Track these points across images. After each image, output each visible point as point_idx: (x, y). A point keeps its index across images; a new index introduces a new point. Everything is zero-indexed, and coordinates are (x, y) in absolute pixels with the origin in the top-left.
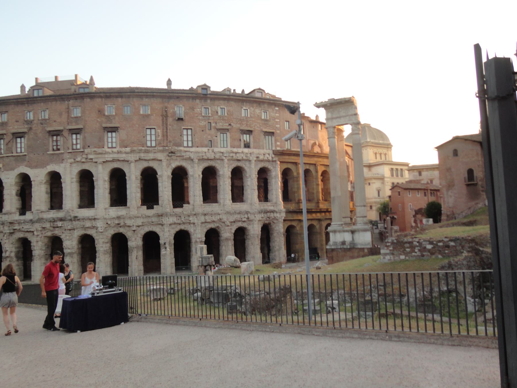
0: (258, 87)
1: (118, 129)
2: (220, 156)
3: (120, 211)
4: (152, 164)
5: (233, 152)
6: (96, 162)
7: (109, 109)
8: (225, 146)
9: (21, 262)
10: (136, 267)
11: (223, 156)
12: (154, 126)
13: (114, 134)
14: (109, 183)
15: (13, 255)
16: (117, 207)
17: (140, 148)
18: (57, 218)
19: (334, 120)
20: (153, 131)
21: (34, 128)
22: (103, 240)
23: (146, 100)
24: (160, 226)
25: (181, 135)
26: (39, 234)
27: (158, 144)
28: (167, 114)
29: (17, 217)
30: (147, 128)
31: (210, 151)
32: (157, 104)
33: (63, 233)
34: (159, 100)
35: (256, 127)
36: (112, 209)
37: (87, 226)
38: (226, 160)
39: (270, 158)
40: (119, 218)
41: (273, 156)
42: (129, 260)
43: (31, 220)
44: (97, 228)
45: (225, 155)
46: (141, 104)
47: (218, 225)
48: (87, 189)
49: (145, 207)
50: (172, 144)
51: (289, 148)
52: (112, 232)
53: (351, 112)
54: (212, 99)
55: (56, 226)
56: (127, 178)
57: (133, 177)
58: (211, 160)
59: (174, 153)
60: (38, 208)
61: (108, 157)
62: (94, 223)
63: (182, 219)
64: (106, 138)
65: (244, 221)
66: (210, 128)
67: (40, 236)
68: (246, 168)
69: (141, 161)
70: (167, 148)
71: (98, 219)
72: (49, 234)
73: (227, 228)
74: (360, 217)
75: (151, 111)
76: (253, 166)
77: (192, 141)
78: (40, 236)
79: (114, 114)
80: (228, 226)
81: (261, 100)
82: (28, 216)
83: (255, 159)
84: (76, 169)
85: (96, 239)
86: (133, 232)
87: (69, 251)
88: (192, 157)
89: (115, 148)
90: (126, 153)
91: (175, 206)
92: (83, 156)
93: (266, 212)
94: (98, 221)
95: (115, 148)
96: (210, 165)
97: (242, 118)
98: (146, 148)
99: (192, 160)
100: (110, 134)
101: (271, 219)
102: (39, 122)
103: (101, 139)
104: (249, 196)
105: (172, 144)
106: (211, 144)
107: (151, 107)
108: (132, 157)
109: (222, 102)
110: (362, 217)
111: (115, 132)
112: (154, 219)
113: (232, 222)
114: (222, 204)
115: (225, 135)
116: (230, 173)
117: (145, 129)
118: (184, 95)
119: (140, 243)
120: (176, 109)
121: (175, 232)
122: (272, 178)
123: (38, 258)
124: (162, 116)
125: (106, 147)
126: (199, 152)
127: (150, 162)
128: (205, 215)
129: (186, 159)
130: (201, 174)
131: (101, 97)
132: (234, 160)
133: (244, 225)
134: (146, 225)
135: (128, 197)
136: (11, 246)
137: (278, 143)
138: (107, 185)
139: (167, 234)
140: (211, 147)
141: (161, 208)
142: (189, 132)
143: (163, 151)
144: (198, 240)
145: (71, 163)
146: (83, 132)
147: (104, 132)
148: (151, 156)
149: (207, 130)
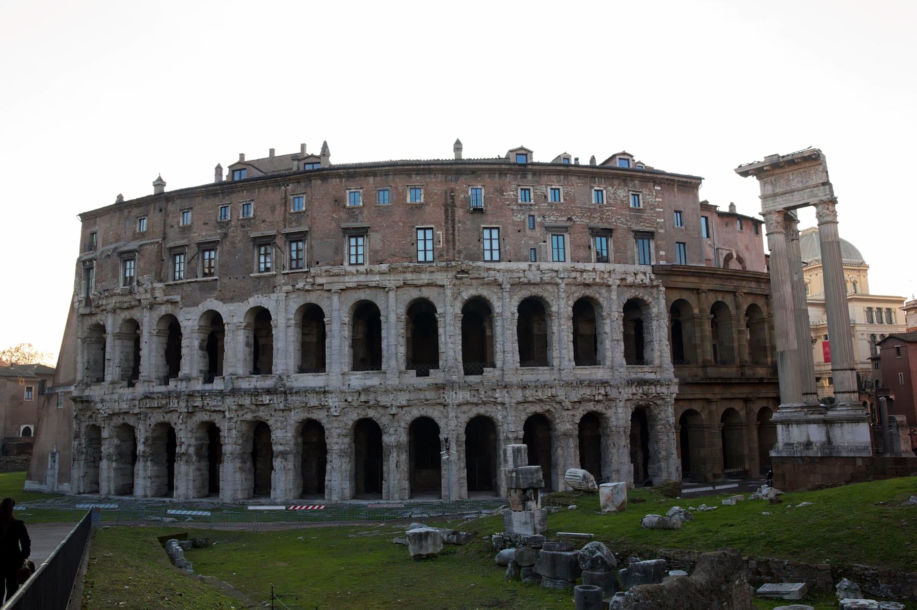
0: (620, 151)
2: (552, 278)
3: (372, 379)
4: (426, 293)
5: (575, 270)
6: (329, 291)
7: (353, 197)
8: (562, 259)
9: (204, 464)
10: (396, 482)
11: (558, 277)
12: (430, 224)
13: (360, 240)
14: (351, 327)
15: (192, 450)
16: (363, 372)
17: (406, 264)
18: (263, 389)
19: (779, 199)
20: (429, 234)
21: (231, 235)
22: (339, 431)
23: (416, 179)
24: (441, 408)
25: (480, 240)
26: (232, 415)
27: (438, 256)
28: (453, 202)
29: (198, 385)
30: (418, 229)
31: (534, 268)
32: (437, 185)
33: (271, 415)
34: (440, 177)
35: (620, 222)
36: (355, 375)
37: (312, 404)
38: (563, 286)
39: (647, 281)
40: (366, 390)
41: (653, 277)
42: (385, 468)
43: (221, 392)
44: (329, 408)
45: (562, 276)
46: (407, 186)
47: (548, 407)
48: (315, 340)
49: (414, 372)
50: (462, 256)
51: (683, 263)
52: (354, 416)
53: (816, 179)
54: (535, 173)
55: (261, 403)
56: (382, 318)
57: (393, 318)
58: (535, 284)
59: (467, 273)
60: (231, 370)
61: (350, 281)
62: (323, 400)
63: (482, 396)
64: (346, 247)
65: (599, 401)
66: (532, 227)
67: (235, 420)
68: (601, 300)
69: (408, 288)
70: (454, 263)
71: (331, 393)
72: (249, 417)
73: (565, 413)
74: (843, 392)
75: (425, 197)
76: (614, 295)
77: (499, 250)
78: (235, 420)
79: (361, 204)
80: (568, 410)
81: (627, 173)
82: (218, 384)
83: (618, 282)
84: (295, 303)
85: (327, 429)
86: (391, 417)
87: (281, 448)
88: (500, 280)
89: (362, 264)
90: (381, 273)
91: (467, 373)
92: (308, 280)
93: (642, 383)
94: (330, 396)
95: (362, 264)
96: (534, 294)
97: (592, 207)
98: (416, 264)
99: (500, 285)
100: (353, 241)
101: (650, 397)
102: (240, 223)
103: (338, 250)
104: (609, 354)
105: (462, 256)
106: (535, 255)
107: (425, 190)
108: (391, 281)
109: (554, 178)
110: (849, 392)
111: (362, 236)
112: (430, 395)
113: (575, 402)
114: (556, 369)
115: (561, 238)
116: (570, 309)
117: (415, 230)
118: (484, 166)
119: (404, 438)
120: (470, 193)
121: (467, 420)
122: (652, 320)
123: (231, 458)
125: (346, 263)
126: (512, 271)
127: (423, 289)
128: (524, 387)
129: (488, 284)
130: (516, 311)
131: (340, 176)
132: (579, 285)
133: (599, 408)
134: (415, 405)
135: (384, 353)
136: (190, 435)
137: (662, 253)
138: (347, 332)
139: (453, 423)
140: (536, 261)
141: (442, 374)
142: (495, 234)
143: (446, 269)
144: (511, 436)
145: (287, 293)
148: (425, 278)
149: (527, 228)
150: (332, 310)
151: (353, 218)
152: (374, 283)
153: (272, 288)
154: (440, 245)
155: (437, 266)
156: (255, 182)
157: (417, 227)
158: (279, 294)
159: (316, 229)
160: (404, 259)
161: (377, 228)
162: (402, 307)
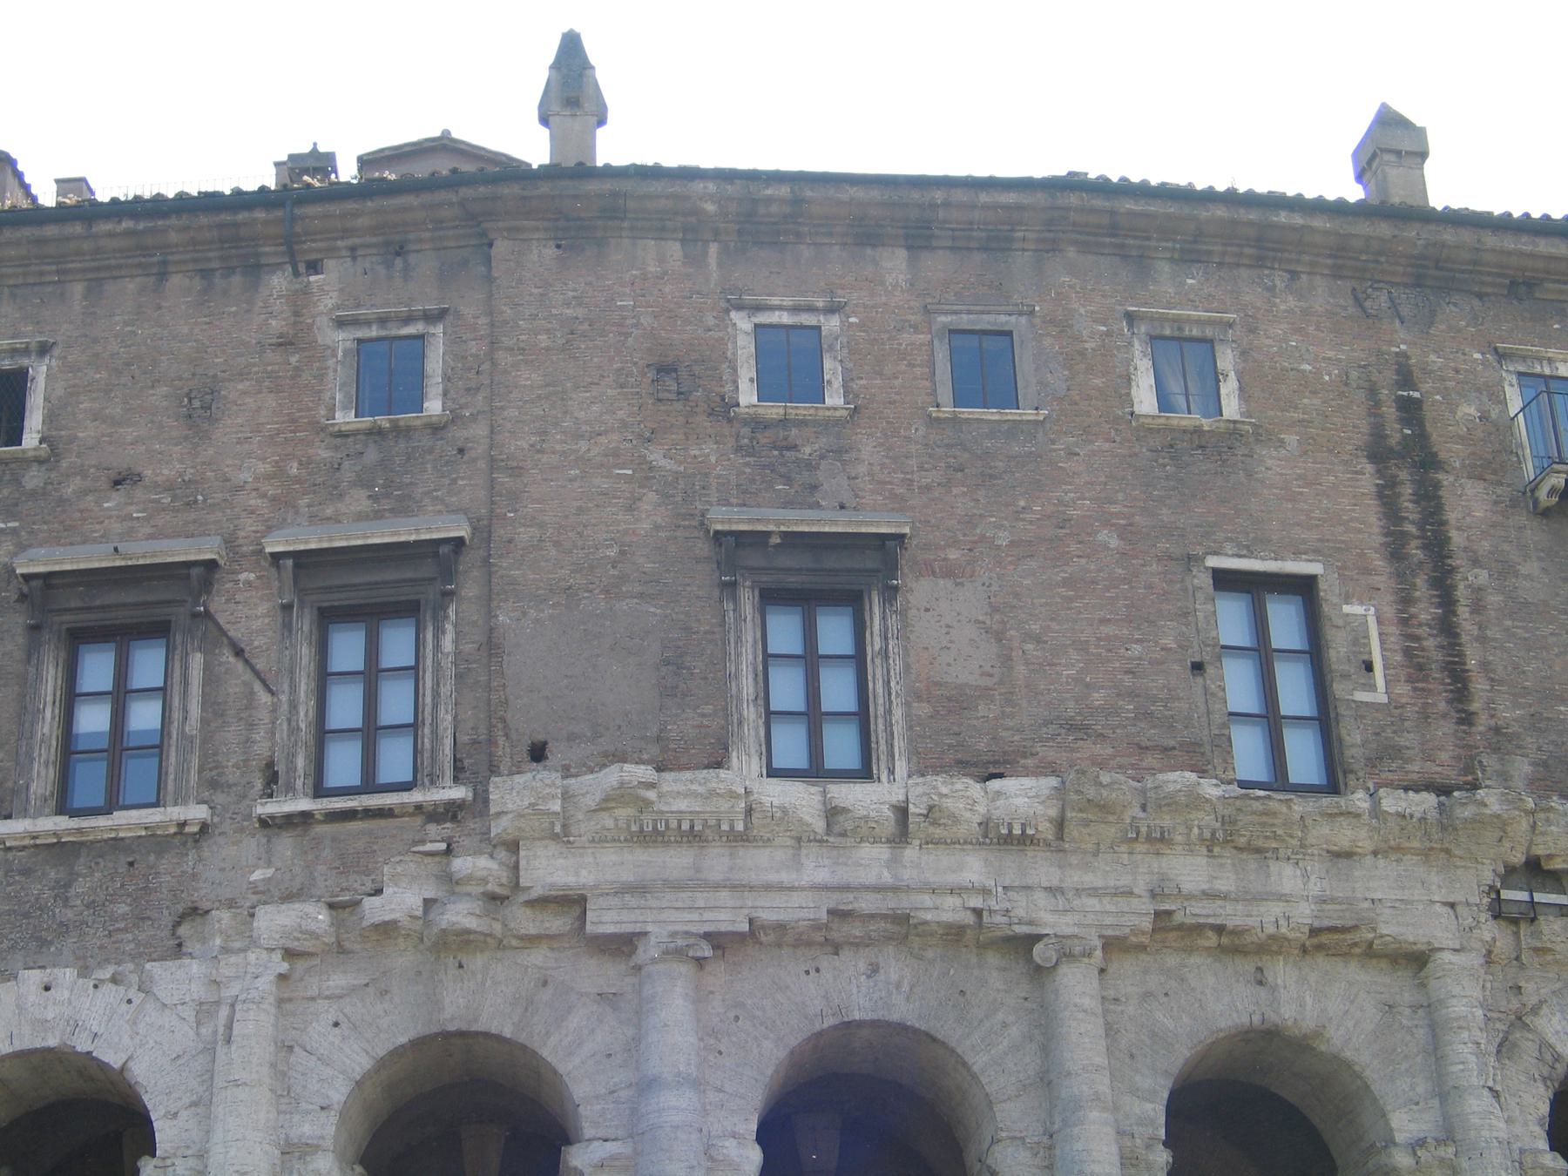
1: (892, 568)
6: (622, 945)
12: (1297, 554)
28: (1422, 437)
46: (1131, 318)
50: (1522, 768)
95: (865, 773)
100: (785, 631)
107: (1244, 354)
111: (853, 601)
117: (1206, 581)
124: (1378, 453)
145: (290, 954)
146: (470, 588)
147: (730, 589)
150: (647, 1086)
151: (788, 480)
152: (951, 901)
153: (167, 919)
154: (1372, 688)
155: (1376, 812)
156: (78, 228)
157: (1213, 562)
158: (229, 966)
159: (525, 535)
160: (1150, 760)
161: (953, 555)
162: (1145, 1082)
